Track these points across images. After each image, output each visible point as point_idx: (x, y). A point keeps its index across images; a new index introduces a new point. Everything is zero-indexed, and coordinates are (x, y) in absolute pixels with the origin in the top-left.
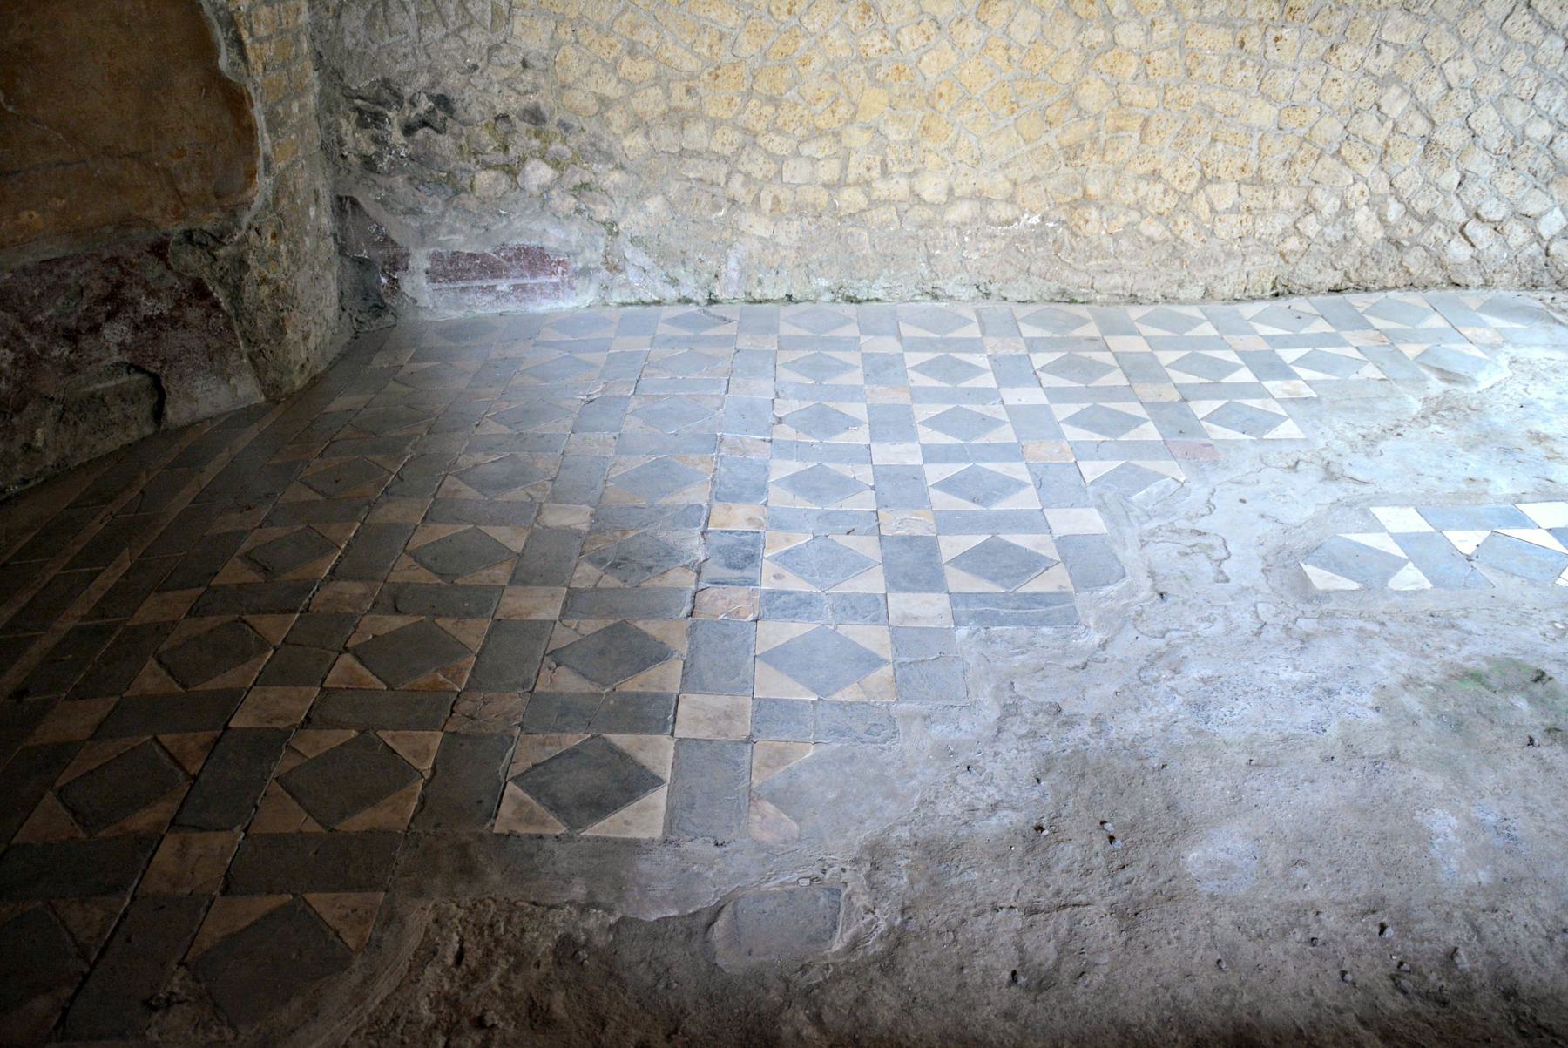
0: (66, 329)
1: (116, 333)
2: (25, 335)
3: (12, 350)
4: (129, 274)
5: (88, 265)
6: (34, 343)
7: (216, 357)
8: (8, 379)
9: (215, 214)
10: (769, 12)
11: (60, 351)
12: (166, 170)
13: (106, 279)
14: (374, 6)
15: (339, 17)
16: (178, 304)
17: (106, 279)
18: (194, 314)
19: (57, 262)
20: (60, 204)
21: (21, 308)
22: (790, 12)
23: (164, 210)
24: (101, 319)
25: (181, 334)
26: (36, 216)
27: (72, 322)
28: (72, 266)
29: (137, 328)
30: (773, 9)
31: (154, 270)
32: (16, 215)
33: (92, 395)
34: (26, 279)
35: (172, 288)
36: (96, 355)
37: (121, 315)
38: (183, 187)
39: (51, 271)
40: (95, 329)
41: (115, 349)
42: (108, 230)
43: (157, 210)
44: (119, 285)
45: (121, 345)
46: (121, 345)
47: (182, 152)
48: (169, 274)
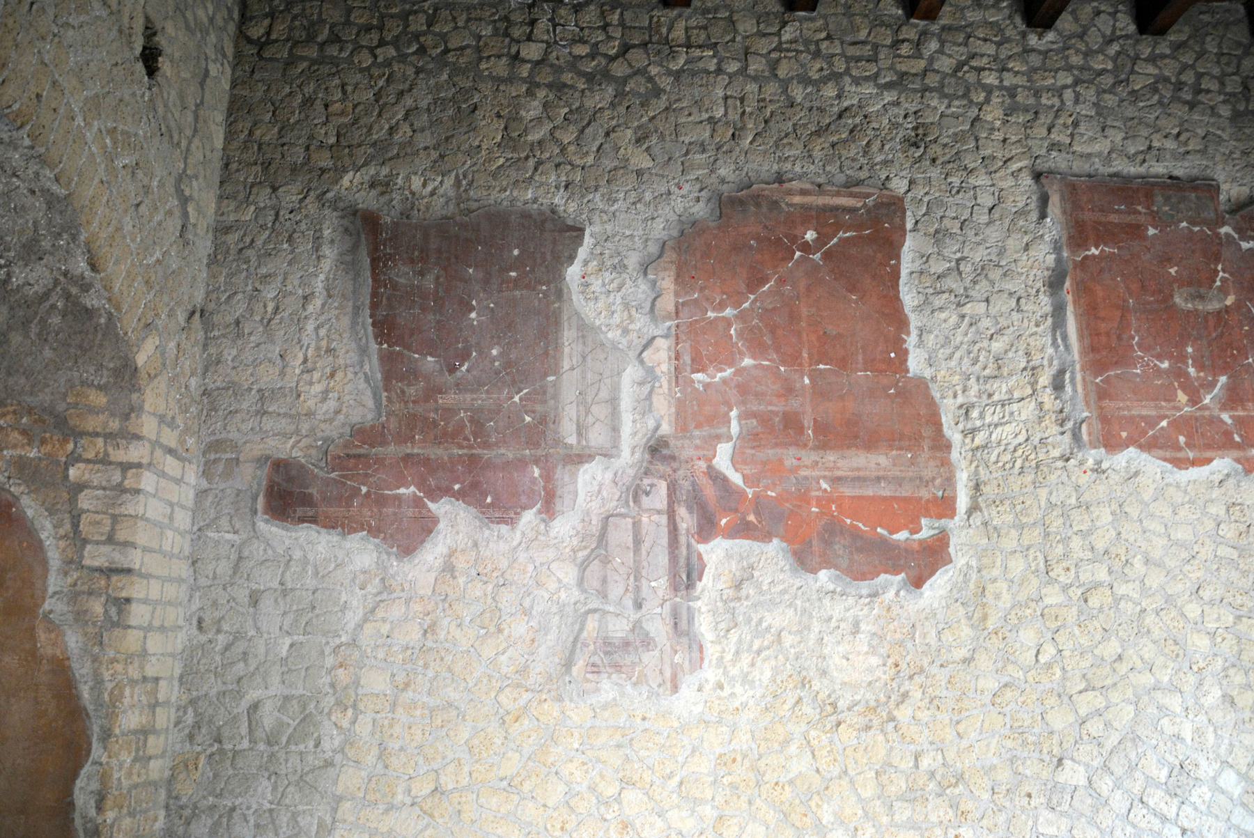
10: (546, 828)
14: (220, 817)
15: (189, 824)
22: (562, 829)
30: (549, 826)
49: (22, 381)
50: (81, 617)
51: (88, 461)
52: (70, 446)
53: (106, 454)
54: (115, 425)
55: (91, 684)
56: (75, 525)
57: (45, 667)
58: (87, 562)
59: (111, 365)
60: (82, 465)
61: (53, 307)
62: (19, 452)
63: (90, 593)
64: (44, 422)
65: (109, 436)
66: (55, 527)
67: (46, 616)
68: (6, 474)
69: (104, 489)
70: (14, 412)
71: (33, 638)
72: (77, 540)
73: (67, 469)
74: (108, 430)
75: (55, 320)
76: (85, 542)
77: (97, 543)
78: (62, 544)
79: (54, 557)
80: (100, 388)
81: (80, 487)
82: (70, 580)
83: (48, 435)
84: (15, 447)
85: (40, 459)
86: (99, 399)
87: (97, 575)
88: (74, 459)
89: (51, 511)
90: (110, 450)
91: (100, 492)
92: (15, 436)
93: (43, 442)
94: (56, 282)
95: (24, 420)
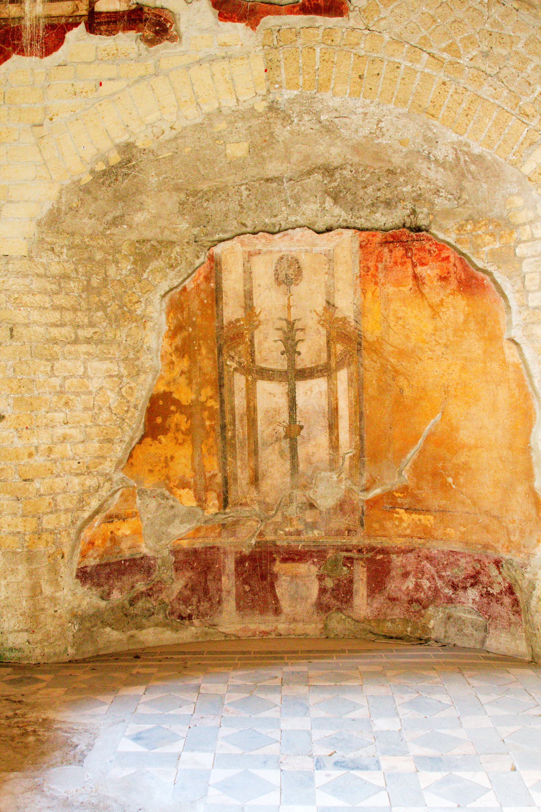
0: (453, 583)
1: (473, 594)
2: (437, 579)
3: (430, 582)
4: (483, 569)
5: (468, 559)
6: (439, 583)
7: (513, 625)
8: (425, 593)
9: (522, 555)
11: (448, 591)
12: (507, 528)
13: (474, 568)
16: (501, 593)
17: (474, 568)
18: (507, 600)
19: (456, 553)
20: (463, 529)
21: (438, 567)
23: (503, 546)
24: (469, 585)
25: (500, 608)
26: (453, 531)
27: (456, 581)
28: (462, 557)
29: (482, 595)
31: (494, 572)
32: (445, 528)
33: (460, 618)
34: (443, 556)
35: (500, 583)
36: (463, 600)
37: (476, 587)
38: (513, 538)
39: (453, 556)
40: (465, 588)
41: (471, 601)
42: (479, 547)
43: (500, 545)
44: (478, 573)
45: (473, 600)
46: (473, 600)
47: (513, 522)
48: (500, 576)
49: (484, 205)
50: (530, 337)
51: (524, 242)
52: (515, 235)
53: (533, 234)
54: (531, 215)
55: (538, 378)
56: (523, 283)
57: (511, 369)
58: (531, 304)
59: (515, 180)
60: (522, 245)
61: (465, 162)
62: (491, 247)
63: (533, 323)
64: (499, 225)
65: (531, 222)
66: (513, 286)
67: (512, 341)
68: (486, 261)
69: (533, 256)
70: (485, 225)
71: (503, 353)
72: (524, 291)
73: (515, 250)
74: (529, 220)
75: (473, 168)
76: (528, 292)
77: (534, 292)
78: (517, 295)
79: (513, 303)
80: (518, 194)
81: (521, 260)
82: (523, 317)
83: (503, 232)
84: (488, 244)
85: (501, 247)
86: (519, 202)
87: (537, 311)
88: (519, 242)
89: (510, 277)
90: (534, 230)
91: (533, 259)
92: (487, 238)
93: (501, 237)
94: (456, 150)
95: (491, 227)
